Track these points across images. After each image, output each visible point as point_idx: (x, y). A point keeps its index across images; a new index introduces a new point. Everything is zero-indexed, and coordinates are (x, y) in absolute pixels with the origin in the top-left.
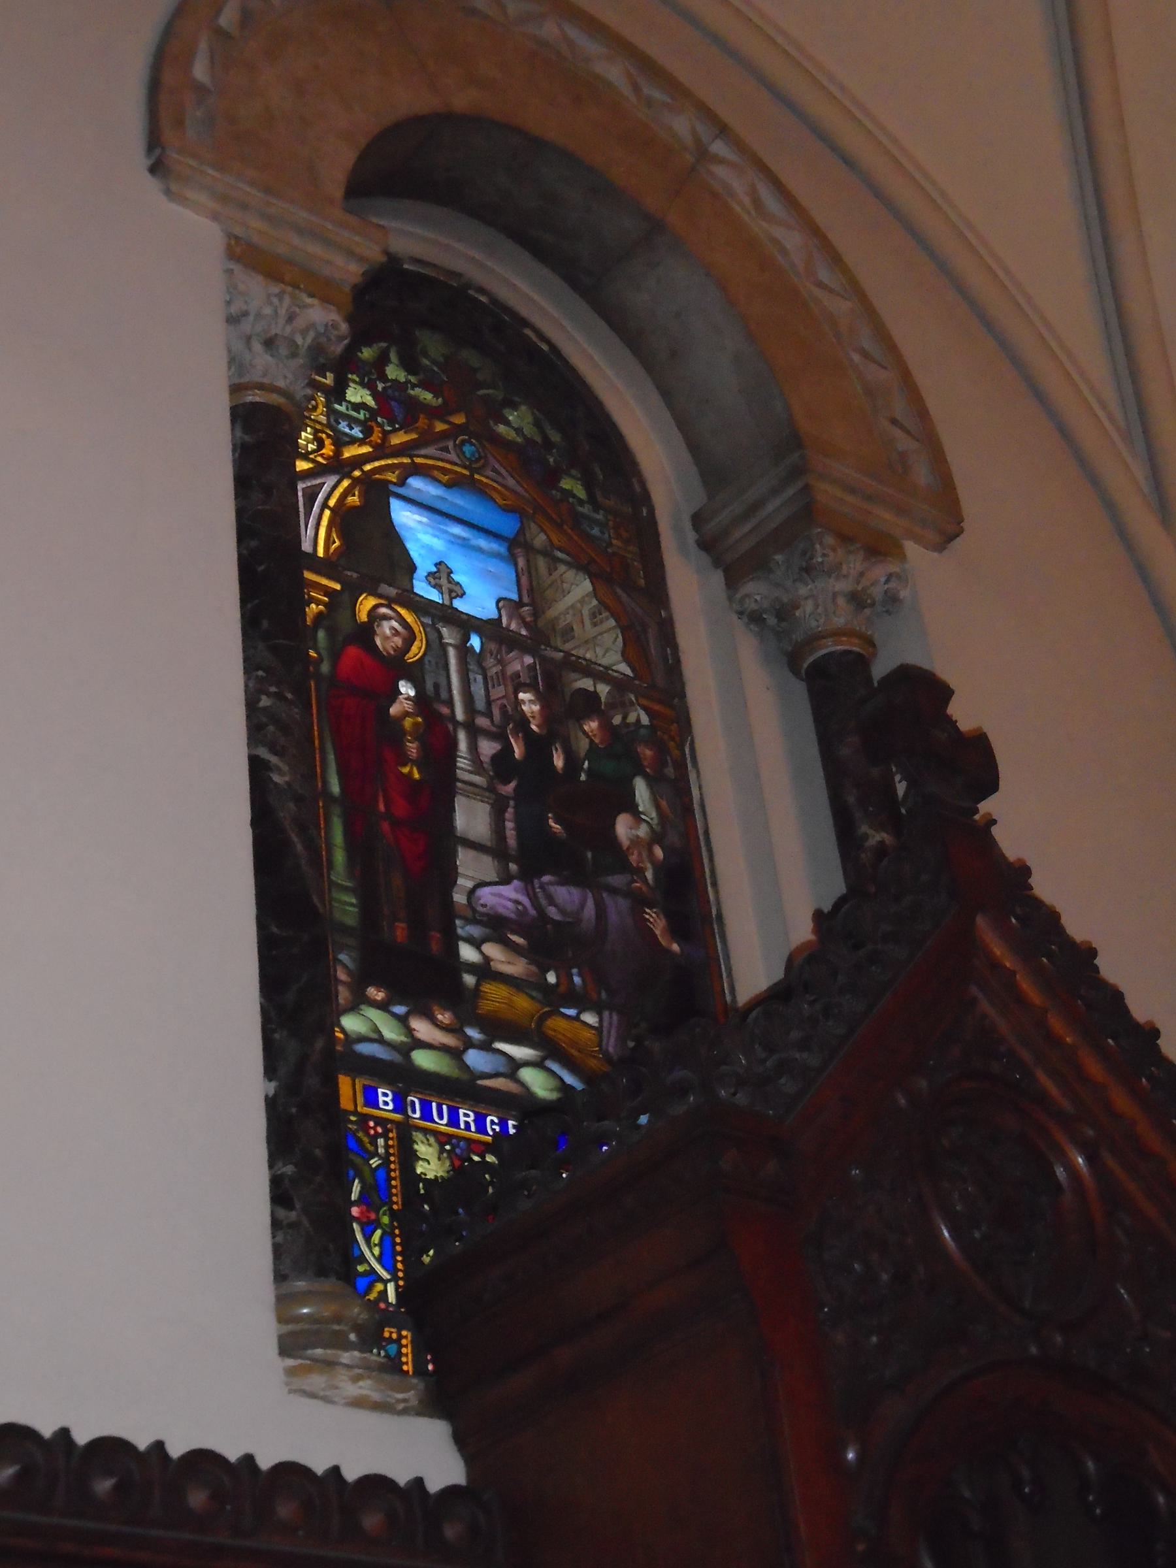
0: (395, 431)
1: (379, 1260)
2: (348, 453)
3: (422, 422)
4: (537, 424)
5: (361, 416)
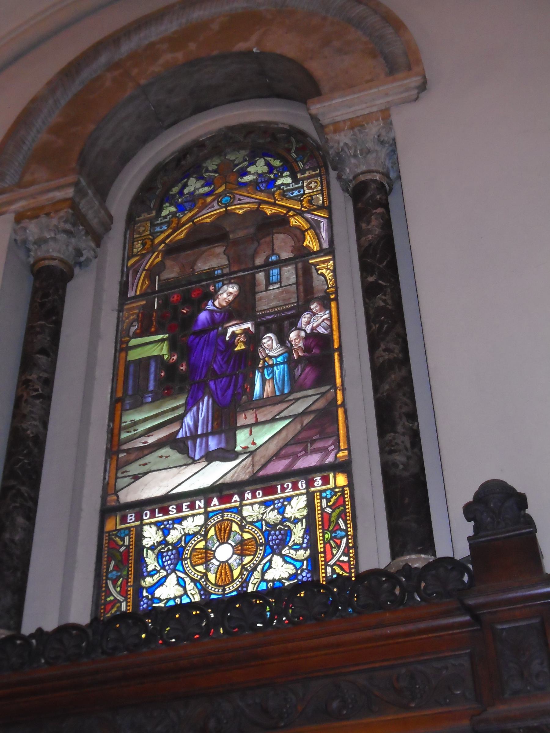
0: (185, 214)
1: (120, 593)
4: (268, 164)
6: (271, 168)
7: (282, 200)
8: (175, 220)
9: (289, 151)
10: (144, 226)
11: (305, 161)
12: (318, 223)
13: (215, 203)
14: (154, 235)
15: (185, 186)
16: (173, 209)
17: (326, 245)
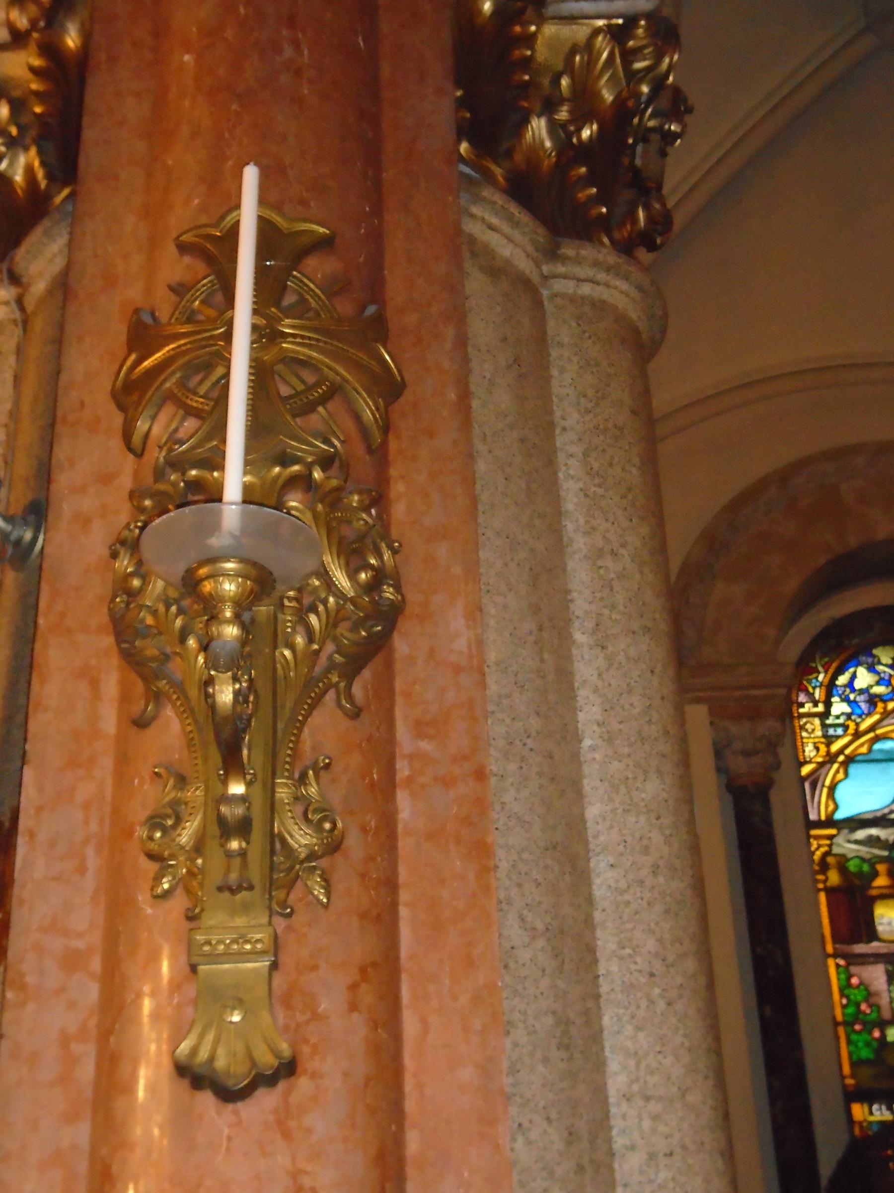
0: (863, 720)
2: (835, 748)
3: (880, 705)
8: (852, 726)
10: (812, 724)
14: (829, 740)
15: (854, 677)
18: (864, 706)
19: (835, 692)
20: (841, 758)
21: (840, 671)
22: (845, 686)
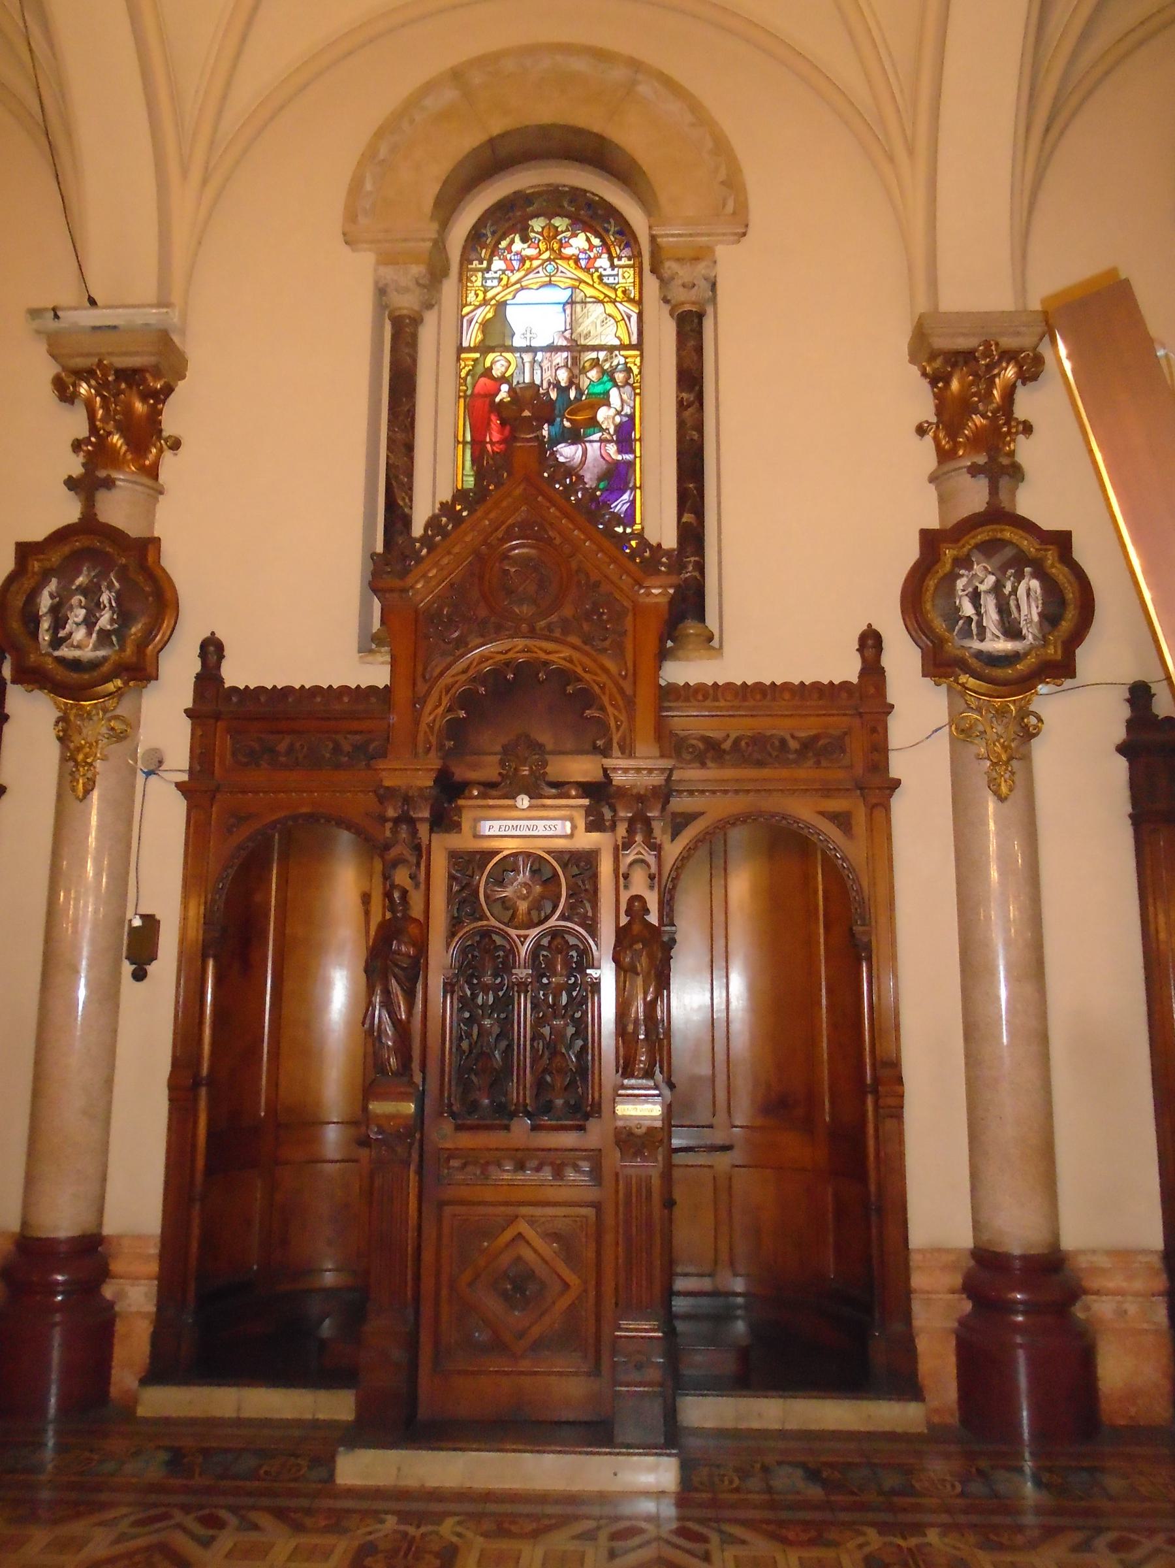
2: (489, 295)
3: (528, 264)
4: (588, 240)
5: (497, 275)
6: (591, 247)
7: (599, 284)
9: (607, 231)
11: (622, 248)
12: (629, 317)
13: (540, 269)
15: (512, 242)
16: (504, 267)
17: (634, 340)
18: (516, 264)
19: (496, 253)
20: (493, 302)
21: (503, 238)
22: (504, 249)
